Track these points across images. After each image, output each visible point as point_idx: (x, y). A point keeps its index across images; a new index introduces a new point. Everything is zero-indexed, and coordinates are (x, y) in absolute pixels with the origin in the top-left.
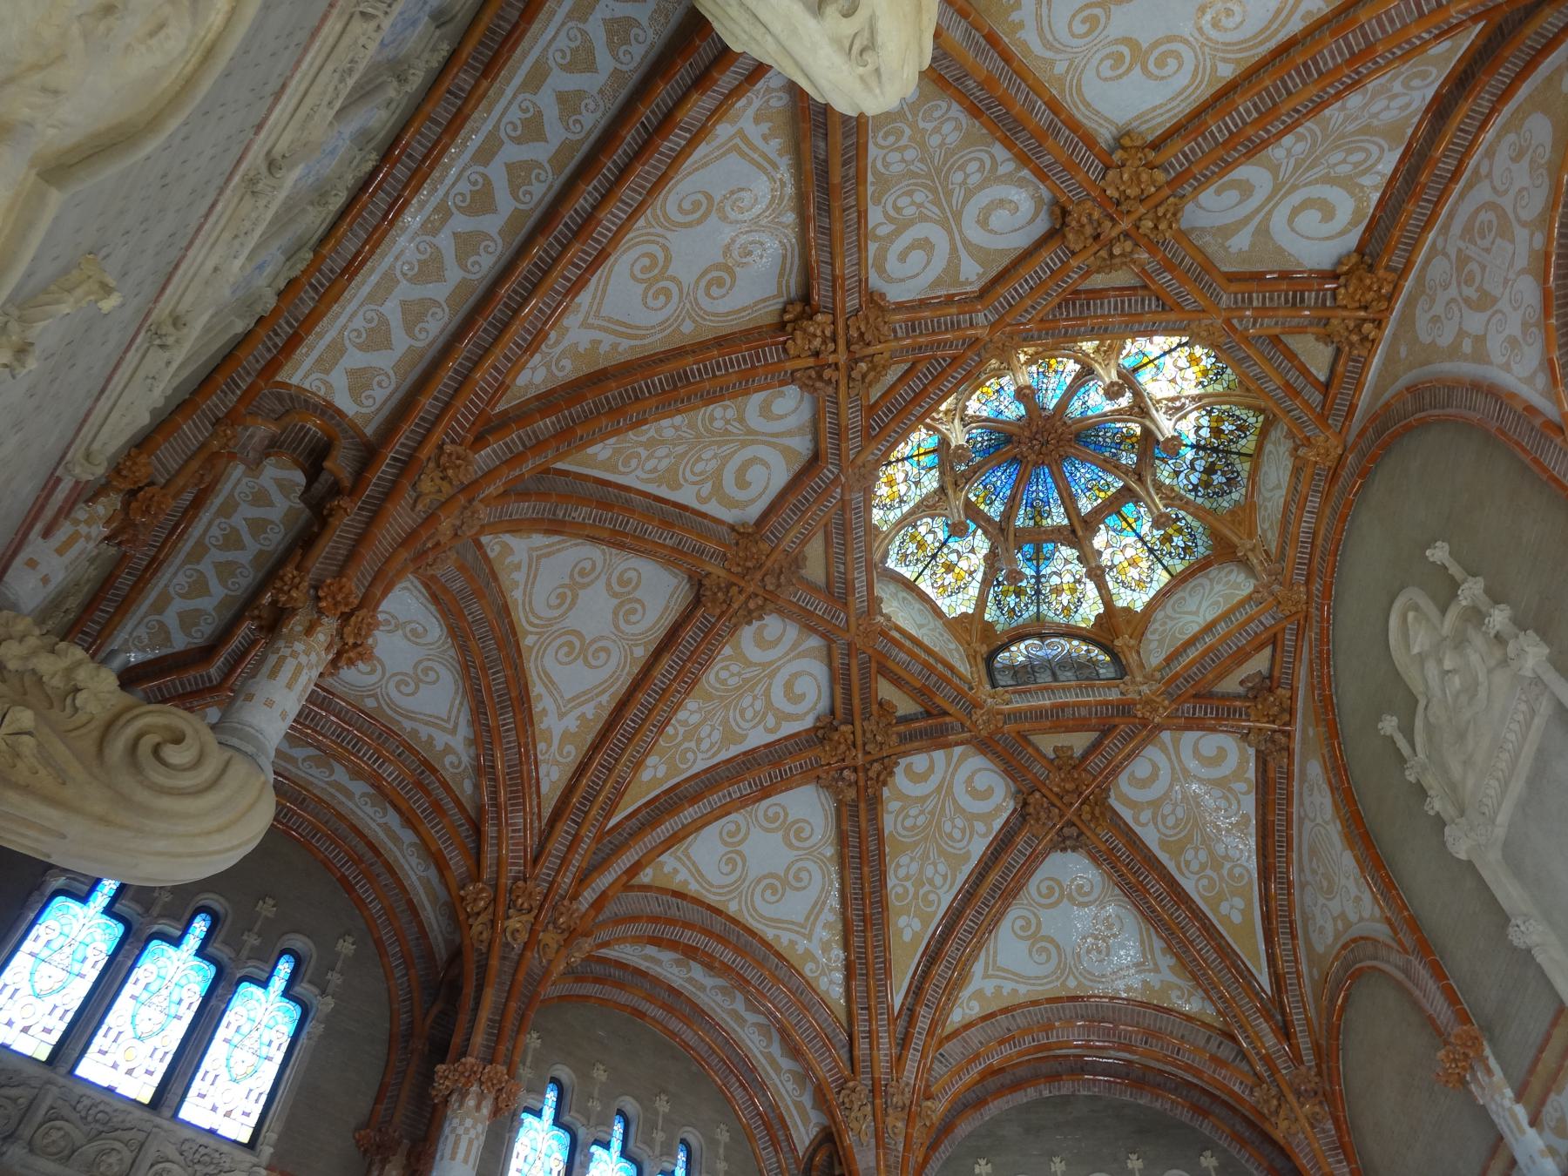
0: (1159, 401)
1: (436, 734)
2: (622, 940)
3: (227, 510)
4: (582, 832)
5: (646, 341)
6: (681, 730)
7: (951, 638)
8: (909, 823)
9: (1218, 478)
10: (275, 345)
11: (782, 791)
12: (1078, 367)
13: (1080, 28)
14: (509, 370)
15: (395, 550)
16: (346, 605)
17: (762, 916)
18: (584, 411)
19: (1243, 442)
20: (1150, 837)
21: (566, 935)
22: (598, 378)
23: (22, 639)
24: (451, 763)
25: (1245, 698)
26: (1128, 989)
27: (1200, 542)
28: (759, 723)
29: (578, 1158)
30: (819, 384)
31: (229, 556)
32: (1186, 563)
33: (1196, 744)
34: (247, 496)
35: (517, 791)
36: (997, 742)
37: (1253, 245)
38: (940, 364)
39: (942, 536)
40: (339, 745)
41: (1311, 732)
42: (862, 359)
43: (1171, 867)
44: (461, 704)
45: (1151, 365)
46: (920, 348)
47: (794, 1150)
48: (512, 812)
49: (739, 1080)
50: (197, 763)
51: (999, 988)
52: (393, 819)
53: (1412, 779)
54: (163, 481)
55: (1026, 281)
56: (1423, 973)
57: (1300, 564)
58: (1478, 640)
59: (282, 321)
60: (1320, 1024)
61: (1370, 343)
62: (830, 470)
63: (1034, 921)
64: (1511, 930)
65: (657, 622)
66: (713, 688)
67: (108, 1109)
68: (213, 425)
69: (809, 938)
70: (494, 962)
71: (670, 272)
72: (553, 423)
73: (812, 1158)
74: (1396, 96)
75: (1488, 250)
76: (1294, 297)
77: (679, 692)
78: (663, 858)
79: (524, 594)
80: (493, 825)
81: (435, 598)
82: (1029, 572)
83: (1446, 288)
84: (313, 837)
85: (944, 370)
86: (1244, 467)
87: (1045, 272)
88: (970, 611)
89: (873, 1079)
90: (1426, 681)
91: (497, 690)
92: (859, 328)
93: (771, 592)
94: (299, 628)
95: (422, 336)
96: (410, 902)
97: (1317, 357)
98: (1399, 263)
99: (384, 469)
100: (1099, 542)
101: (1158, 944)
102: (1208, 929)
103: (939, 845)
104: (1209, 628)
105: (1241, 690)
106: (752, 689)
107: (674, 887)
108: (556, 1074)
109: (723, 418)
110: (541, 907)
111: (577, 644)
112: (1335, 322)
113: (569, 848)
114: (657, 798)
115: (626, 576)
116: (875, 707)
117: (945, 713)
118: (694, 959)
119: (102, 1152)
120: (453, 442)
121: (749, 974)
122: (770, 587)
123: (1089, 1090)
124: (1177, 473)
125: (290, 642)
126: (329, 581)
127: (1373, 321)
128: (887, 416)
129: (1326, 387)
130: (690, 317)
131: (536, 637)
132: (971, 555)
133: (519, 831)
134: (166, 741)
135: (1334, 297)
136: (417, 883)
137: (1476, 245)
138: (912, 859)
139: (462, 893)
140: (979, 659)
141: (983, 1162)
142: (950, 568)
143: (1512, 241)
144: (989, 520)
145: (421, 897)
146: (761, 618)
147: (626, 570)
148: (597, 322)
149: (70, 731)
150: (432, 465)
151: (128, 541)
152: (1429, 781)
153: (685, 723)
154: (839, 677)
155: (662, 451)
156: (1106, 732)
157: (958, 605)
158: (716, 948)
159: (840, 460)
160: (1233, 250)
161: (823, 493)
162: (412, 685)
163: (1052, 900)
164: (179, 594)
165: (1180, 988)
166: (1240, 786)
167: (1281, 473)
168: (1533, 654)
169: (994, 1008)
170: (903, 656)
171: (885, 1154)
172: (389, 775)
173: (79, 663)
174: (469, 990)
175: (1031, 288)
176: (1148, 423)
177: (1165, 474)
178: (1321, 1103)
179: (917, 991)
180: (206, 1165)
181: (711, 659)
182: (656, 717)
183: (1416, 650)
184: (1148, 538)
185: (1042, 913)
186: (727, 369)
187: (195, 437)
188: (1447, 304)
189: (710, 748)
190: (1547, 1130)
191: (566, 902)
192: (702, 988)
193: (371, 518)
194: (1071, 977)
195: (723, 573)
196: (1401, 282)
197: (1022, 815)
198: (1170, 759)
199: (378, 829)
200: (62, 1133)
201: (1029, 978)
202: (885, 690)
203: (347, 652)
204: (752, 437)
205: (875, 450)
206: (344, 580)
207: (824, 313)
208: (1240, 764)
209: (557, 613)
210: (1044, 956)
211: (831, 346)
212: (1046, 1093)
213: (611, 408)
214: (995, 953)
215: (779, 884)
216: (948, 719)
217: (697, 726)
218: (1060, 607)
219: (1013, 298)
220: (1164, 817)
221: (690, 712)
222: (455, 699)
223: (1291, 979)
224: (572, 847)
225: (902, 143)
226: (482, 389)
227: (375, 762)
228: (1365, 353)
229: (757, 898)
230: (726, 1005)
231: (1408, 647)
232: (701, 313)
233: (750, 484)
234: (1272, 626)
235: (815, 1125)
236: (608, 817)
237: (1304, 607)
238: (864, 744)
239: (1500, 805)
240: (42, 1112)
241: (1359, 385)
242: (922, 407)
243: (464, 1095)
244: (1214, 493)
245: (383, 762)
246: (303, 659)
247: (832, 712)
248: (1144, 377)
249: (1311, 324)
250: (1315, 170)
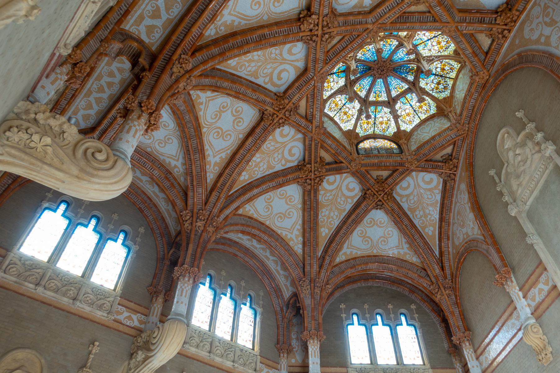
0: (424, 57)
1: (172, 161)
2: (231, 231)
3: (99, 78)
4: (221, 196)
5: (250, 22)
6: (254, 164)
7: (345, 138)
8: (326, 198)
9: (441, 86)
10: (121, 14)
11: (286, 186)
12: (397, 43)
14: (204, 28)
15: (165, 92)
16: (151, 109)
17: (277, 226)
18: (229, 46)
19: (451, 74)
20: (405, 206)
21: (215, 229)
22: (233, 35)
23: (44, 113)
24: (177, 171)
25: (442, 162)
26: (393, 254)
27: (432, 109)
28: (280, 163)
29: (217, 298)
30: (311, 42)
31: (100, 95)
32: (426, 116)
33: (424, 177)
34: (106, 73)
35: (199, 181)
36: (358, 173)
38: (353, 37)
39: (344, 102)
40: (139, 163)
41: (463, 174)
42: (327, 33)
43: (411, 216)
44: (180, 151)
45: (423, 44)
46: (347, 31)
47: (283, 299)
48: (198, 188)
49: (267, 277)
50: (107, 160)
51: (352, 252)
52: (156, 189)
53: (499, 190)
54: (85, 61)
55: (388, 7)
56: (493, 251)
57: (467, 117)
58: (530, 144)
59: (123, 5)
60: (454, 267)
62: (310, 74)
63: (364, 232)
64: (527, 238)
65: (247, 126)
66: (265, 150)
67: (68, 277)
68: (100, 42)
69: (292, 233)
70: (193, 236)
72: (218, 50)
73: (289, 301)
76: (481, 19)
77: (254, 150)
78: (246, 206)
79: (204, 114)
80: (192, 192)
81: (174, 112)
82: (373, 116)
83: (537, 18)
84: (129, 194)
85: (354, 39)
86: (450, 83)
87: (395, 4)
88: (351, 129)
89: (311, 278)
90: (508, 157)
91: (194, 146)
92: (327, 21)
93: (287, 117)
94: (135, 117)
95: (172, 14)
96: (162, 217)
97: (485, 41)
98: (521, 8)
99: (159, 63)
100: (397, 106)
101: (404, 240)
102: (421, 236)
103: (335, 206)
104: (433, 138)
105: (441, 159)
106: (278, 151)
107: (249, 215)
108: (210, 272)
109: (275, 53)
110: (208, 219)
111: (221, 132)
112: (494, 29)
113: (217, 201)
114: (245, 186)
115: (238, 109)
116: (319, 159)
117: (342, 162)
118: (255, 239)
119: (68, 290)
120: (184, 54)
121: (272, 244)
122: (287, 116)
123: (377, 284)
124: (427, 84)
125: (133, 120)
126: (145, 101)
127: (508, 30)
128: (332, 56)
129: (487, 53)
130: (267, 14)
132: (353, 109)
133: (200, 194)
134: (96, 152)
135: (496, 20)
136: (164, 211)
138: (327, 210)
139: (181, 214)
140: (354, 145)
141: (343, 304)
142: (345, 113)
144: (360, 97)
145: (166, 215)
146: (283, 126)
147: (238, 107)
149: (63, 146)
150: (177, 62)
151: (73, 83)
152: (505, 191)
153: (255, 161)
154: (307, 148)
155: (253, 64)
156: (394, 171)
157: (347, 126)
158: (262, 235)
159: (315, 71)
161: (307, 82)
162: (164, 144)
163: (371, 225)
164: (82, 109)
165: (409, 254)
166: (437, 191)
167: (464, 85)
168: (550, 149)
169: (350, 258)
170: (330, 142)
171: (314, 300)
172: (156, 174)
173: (64, 123)
174: (184, 244)
175: (389, 10)
176: (419, 65)
177: (422, 84)
178: (451, 290)
179: (326, 251)
180: (101, 295)
181: (265, 140)
182: (246, 159)
183: (506, 147)
184: (414, 106)
185: (367, 229)
186: (279, 34)
187: (95, 46)
188: (538, 24)
189: (263, 170)
190: (529, 299)
191: (216, 218)
192: (256, 248)
193: (157, 80)
194: (375, 250)
195: (271, 110)
196: (521, 16)
197: (364, 197)
198: (414, 181)
199: (151, 193)
200: (54, 284)
201: (362, 249)
202: (323, 153)
203: (151, 126)
204: (284, 61)
205: (327, 68)
206: (150, 101)
207: (315, 14)
208: (437, 183)
209: (214, 121)
210: (367, 242)
211: (317, 28)
212: (363, 285)
213: (238, 46)
214: (351, 241)
215: (283, 216)
216: (343, 165)
217: (259, 162)
218: (382, 129)
219: (382, 13)
220: (410, 200)
221: (257, 158)
222: (178, 149)
223: (446, 253)
224: (217, 200)
226: (194, 35)
227: (151, 169)
228: (502, 42)
229: (276, 220)
230: (264, 254)
231: (504, 147)
232: (271, 12)
233: (282, 78)
234: (455, 138)
235: (291, 291)
236: (229, 191)
237: (467, 132)
238: (314, 171)
239: (529, 199)
240: (48, 276)
241: (498, 53)
242: (345, 53)
243: (184, 276)
244: (439, 91)
245: (154, 170)
246: (137, 127)
247: (304, 160)
248: (420, 48)
249: (485, 30)
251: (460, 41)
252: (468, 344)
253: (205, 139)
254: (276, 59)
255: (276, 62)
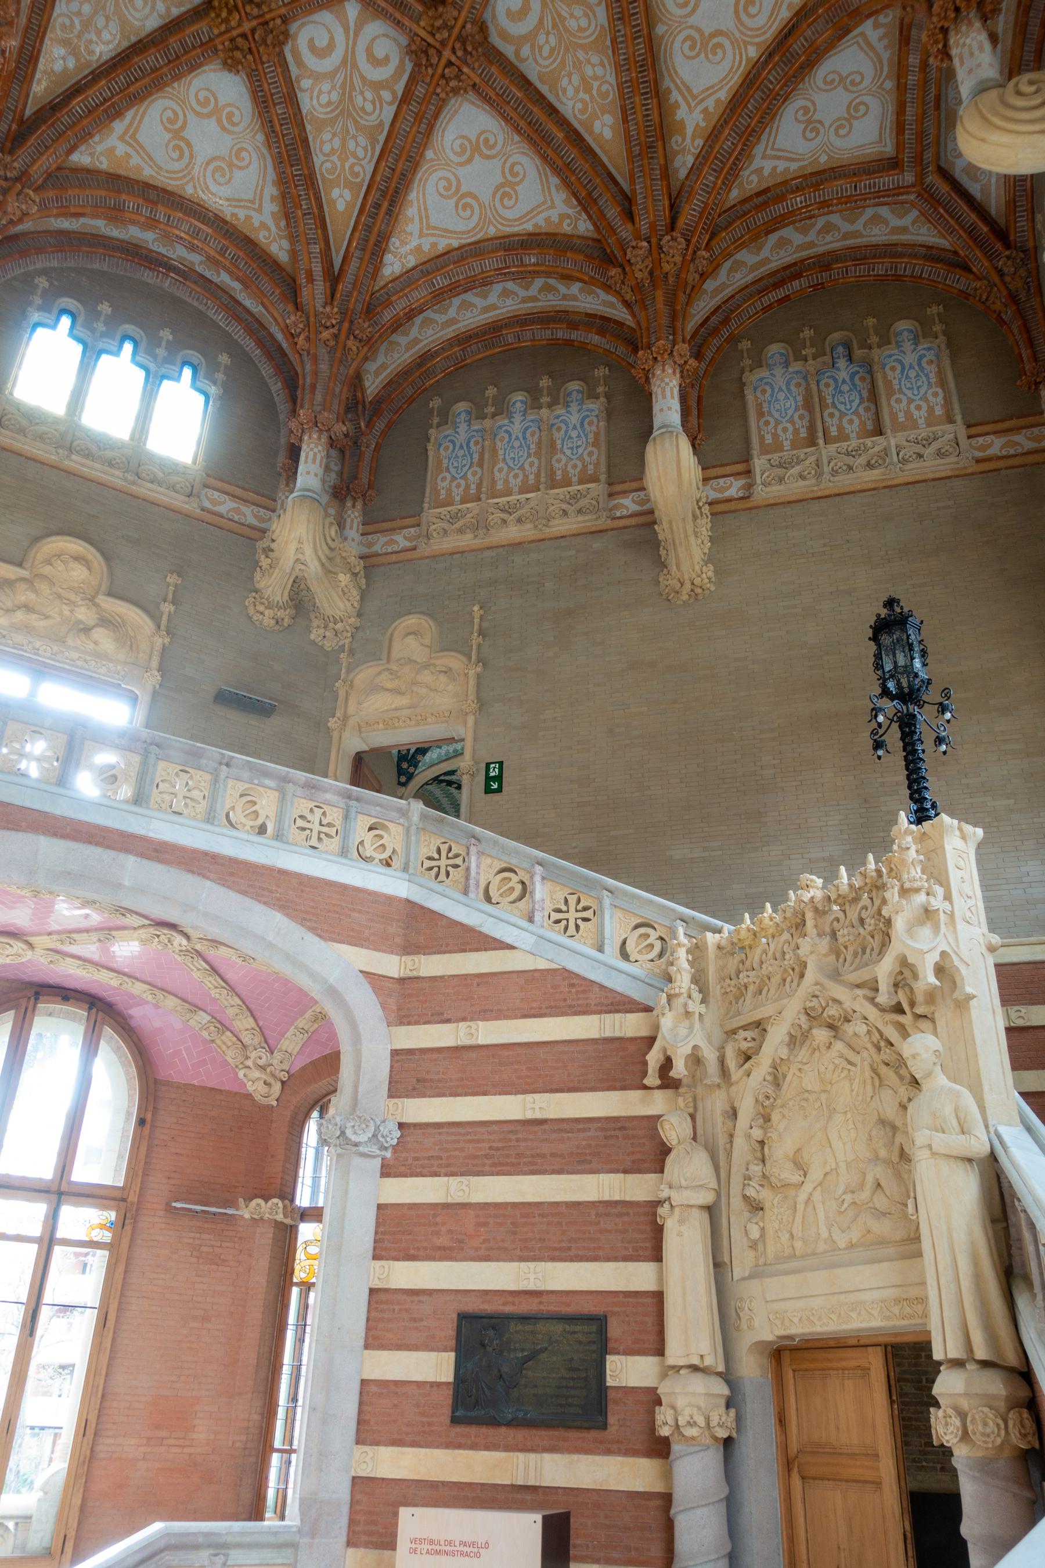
13: (244, 154)
71: (502, 180)
74: (79, 13)
79: (720, 89)
131: (749, 47)
148: (548, 198)
225: (352, 160)
253: (769, 35)
254: (555, 26)
255: (560, 15)
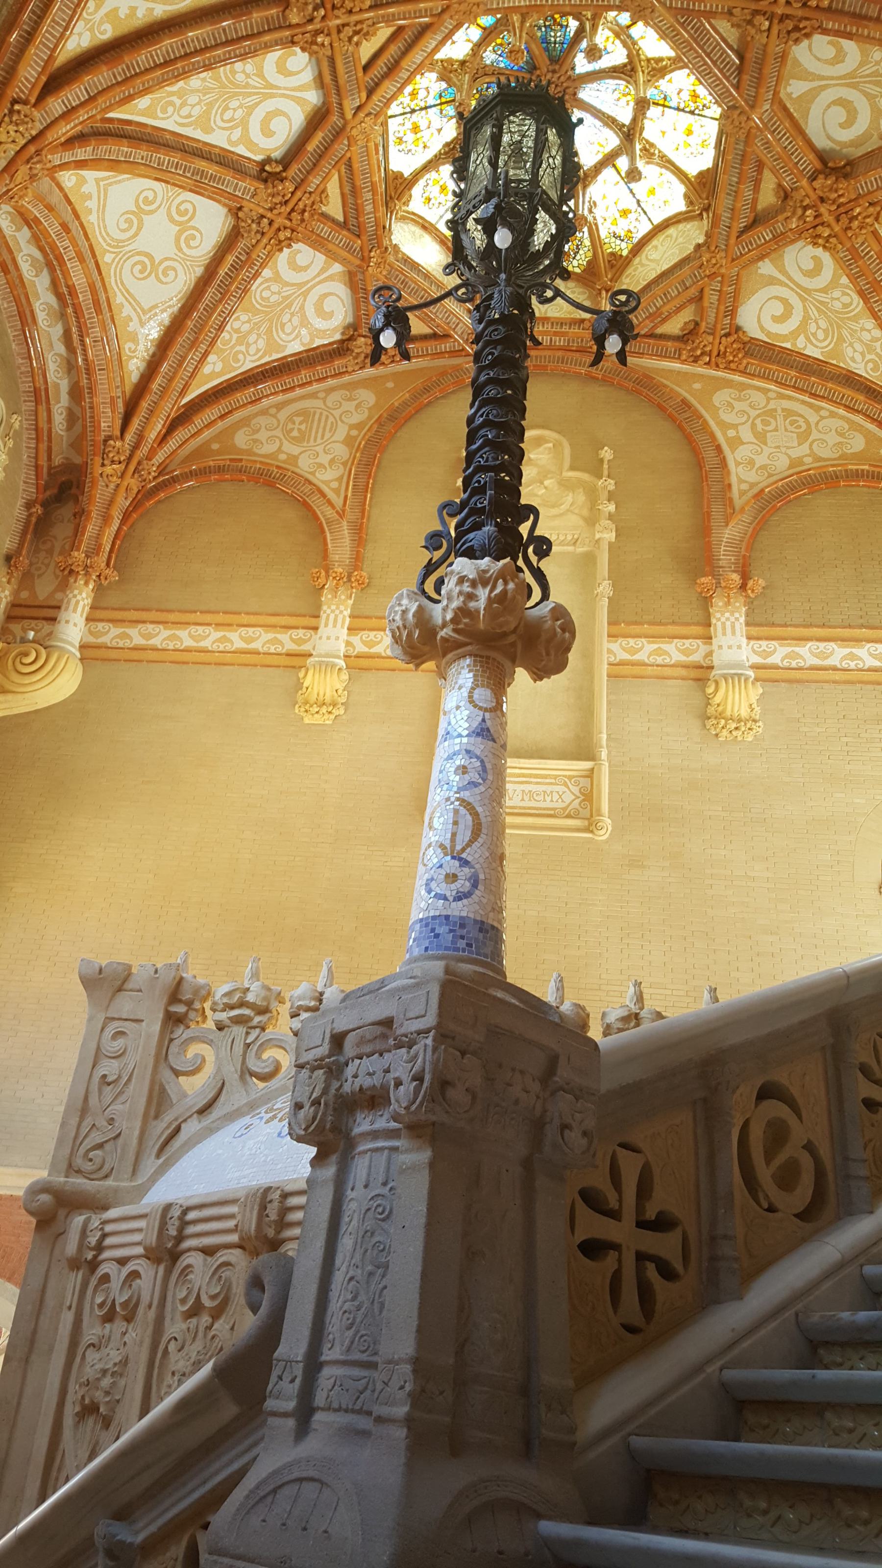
37: (762, 275)
51: (89, 197)
61: (696, 360)
74: (863, 354)
75: (786, 430)
112: (710, 338)
137: (785, 420)
143: (799, 445)
160: (760, 264)
163: (177, 218)
214: (120, 181)
250: (816, 312)
251: (685, 285)
252: (91, 587)
